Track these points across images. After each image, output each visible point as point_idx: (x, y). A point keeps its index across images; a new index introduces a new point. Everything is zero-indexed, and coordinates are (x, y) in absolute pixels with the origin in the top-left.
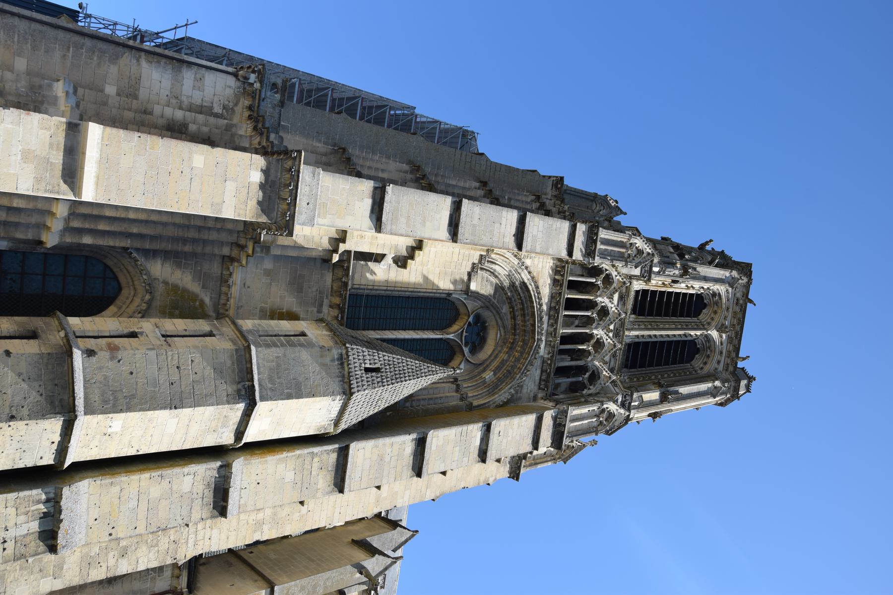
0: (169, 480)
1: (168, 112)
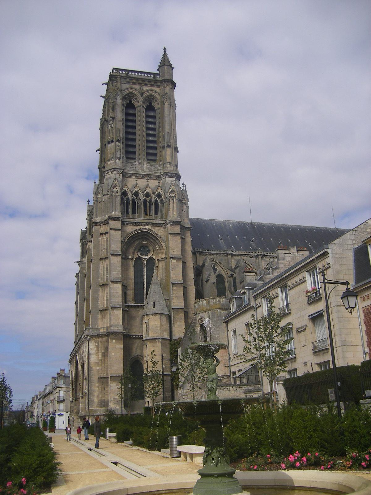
1: (100, 356)
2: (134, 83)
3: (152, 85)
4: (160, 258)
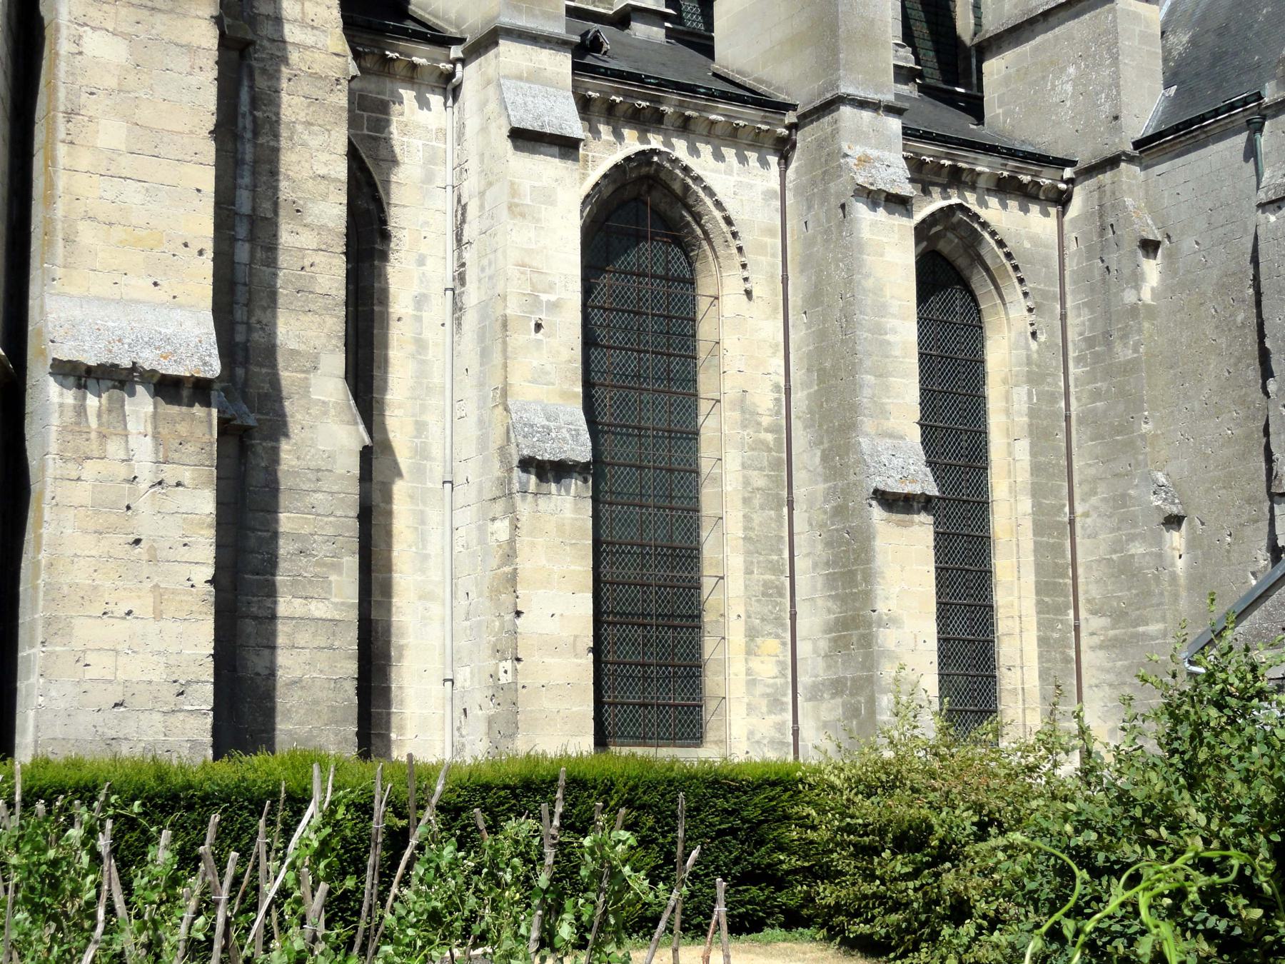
0: (84, 96)
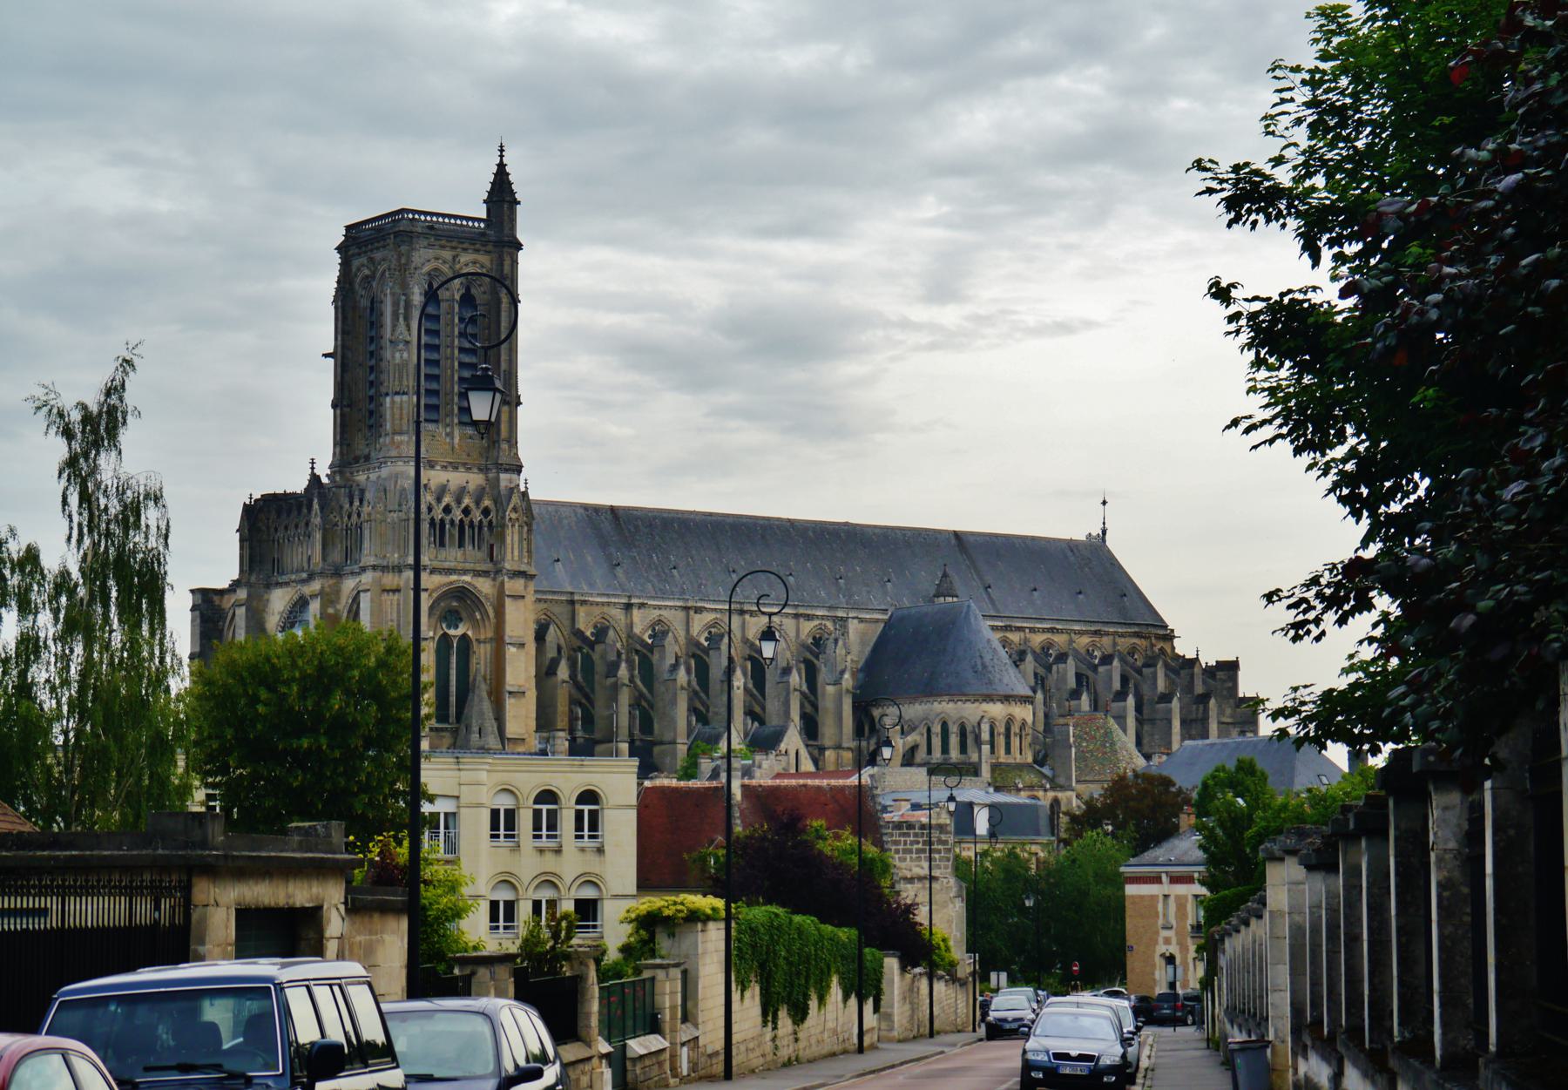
2: (443, 247)
3: (477, 251)
4: (482, 637)
